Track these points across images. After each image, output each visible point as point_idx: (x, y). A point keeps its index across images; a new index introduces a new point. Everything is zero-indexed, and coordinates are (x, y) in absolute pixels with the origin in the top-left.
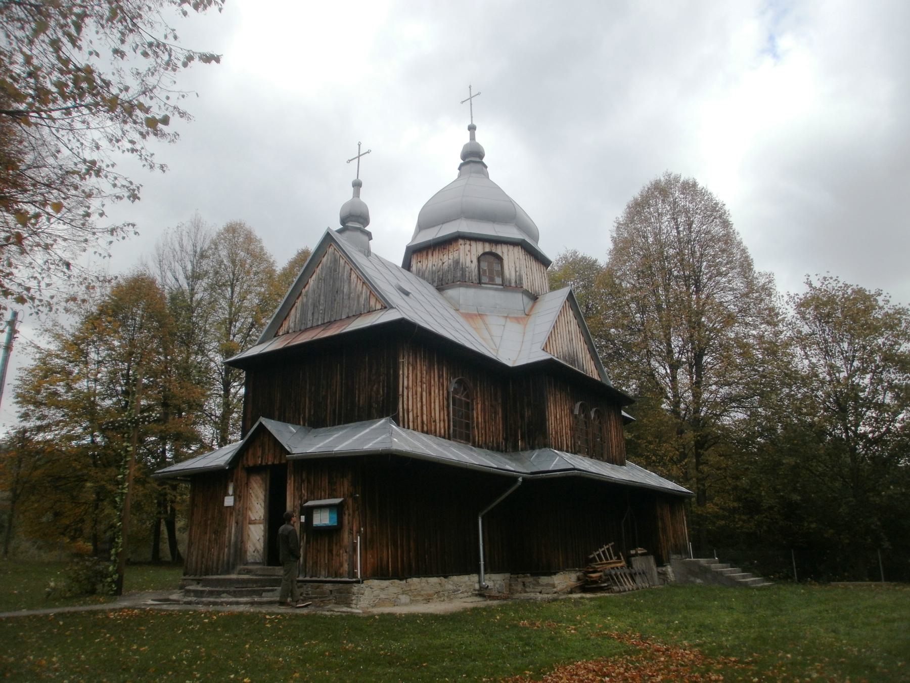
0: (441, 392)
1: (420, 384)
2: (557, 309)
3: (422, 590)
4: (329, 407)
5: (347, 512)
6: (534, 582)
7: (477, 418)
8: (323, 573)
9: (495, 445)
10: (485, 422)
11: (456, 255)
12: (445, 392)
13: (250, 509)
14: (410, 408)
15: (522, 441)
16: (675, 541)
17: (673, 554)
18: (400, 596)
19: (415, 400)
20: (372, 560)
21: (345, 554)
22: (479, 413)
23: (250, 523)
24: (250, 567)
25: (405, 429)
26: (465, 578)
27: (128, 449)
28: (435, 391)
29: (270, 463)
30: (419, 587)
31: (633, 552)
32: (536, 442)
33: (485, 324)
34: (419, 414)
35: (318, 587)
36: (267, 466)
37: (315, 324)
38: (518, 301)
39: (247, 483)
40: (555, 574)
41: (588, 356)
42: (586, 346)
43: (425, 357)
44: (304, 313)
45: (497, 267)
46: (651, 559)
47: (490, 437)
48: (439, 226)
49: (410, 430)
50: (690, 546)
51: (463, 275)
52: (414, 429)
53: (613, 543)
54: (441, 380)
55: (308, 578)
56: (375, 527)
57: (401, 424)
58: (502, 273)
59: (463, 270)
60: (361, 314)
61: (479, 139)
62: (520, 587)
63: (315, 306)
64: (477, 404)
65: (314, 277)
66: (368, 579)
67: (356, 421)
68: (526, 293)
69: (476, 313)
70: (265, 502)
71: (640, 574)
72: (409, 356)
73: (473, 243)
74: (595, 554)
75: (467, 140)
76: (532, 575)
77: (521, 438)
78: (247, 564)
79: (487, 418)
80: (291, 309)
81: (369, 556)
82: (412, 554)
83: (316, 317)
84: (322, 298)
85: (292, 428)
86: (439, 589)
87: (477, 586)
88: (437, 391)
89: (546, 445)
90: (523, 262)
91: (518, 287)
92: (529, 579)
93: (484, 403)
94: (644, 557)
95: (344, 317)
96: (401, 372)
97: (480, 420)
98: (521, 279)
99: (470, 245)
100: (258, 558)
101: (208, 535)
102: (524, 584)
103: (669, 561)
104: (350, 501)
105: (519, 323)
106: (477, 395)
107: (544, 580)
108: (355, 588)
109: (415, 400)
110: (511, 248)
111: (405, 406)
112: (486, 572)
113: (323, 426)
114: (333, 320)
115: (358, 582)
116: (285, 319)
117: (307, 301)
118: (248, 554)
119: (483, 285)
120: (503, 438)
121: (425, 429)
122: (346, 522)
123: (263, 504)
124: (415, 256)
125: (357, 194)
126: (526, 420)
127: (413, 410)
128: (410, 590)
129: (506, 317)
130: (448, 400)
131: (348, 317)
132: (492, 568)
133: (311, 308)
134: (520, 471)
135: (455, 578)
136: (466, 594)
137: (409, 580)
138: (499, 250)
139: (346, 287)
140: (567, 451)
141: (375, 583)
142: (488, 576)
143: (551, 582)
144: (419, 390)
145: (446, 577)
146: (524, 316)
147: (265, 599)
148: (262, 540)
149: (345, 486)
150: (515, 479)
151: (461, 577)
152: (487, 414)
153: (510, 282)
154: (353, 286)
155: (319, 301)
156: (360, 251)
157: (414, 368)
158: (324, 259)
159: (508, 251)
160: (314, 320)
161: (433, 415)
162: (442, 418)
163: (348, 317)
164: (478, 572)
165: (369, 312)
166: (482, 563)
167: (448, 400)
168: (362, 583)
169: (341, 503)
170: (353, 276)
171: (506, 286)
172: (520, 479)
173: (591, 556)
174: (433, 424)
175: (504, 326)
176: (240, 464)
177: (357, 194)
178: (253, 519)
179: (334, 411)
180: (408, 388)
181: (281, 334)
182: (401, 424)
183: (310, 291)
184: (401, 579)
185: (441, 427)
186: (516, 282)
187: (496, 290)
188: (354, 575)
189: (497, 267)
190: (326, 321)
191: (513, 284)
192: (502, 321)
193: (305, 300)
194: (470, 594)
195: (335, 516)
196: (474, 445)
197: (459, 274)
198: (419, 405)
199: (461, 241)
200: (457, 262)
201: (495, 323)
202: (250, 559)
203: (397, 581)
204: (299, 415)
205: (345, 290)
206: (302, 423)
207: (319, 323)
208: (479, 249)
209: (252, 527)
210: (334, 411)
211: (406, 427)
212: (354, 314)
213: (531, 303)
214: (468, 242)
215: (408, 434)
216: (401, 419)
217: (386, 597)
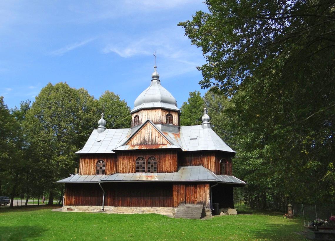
14: (83, 170)
26: (98, 207)
96: (80, 163)
111: (81, 170)
112: (106, 205)
135: (94, 206)
203: (75, 206)
211: (81, 174)
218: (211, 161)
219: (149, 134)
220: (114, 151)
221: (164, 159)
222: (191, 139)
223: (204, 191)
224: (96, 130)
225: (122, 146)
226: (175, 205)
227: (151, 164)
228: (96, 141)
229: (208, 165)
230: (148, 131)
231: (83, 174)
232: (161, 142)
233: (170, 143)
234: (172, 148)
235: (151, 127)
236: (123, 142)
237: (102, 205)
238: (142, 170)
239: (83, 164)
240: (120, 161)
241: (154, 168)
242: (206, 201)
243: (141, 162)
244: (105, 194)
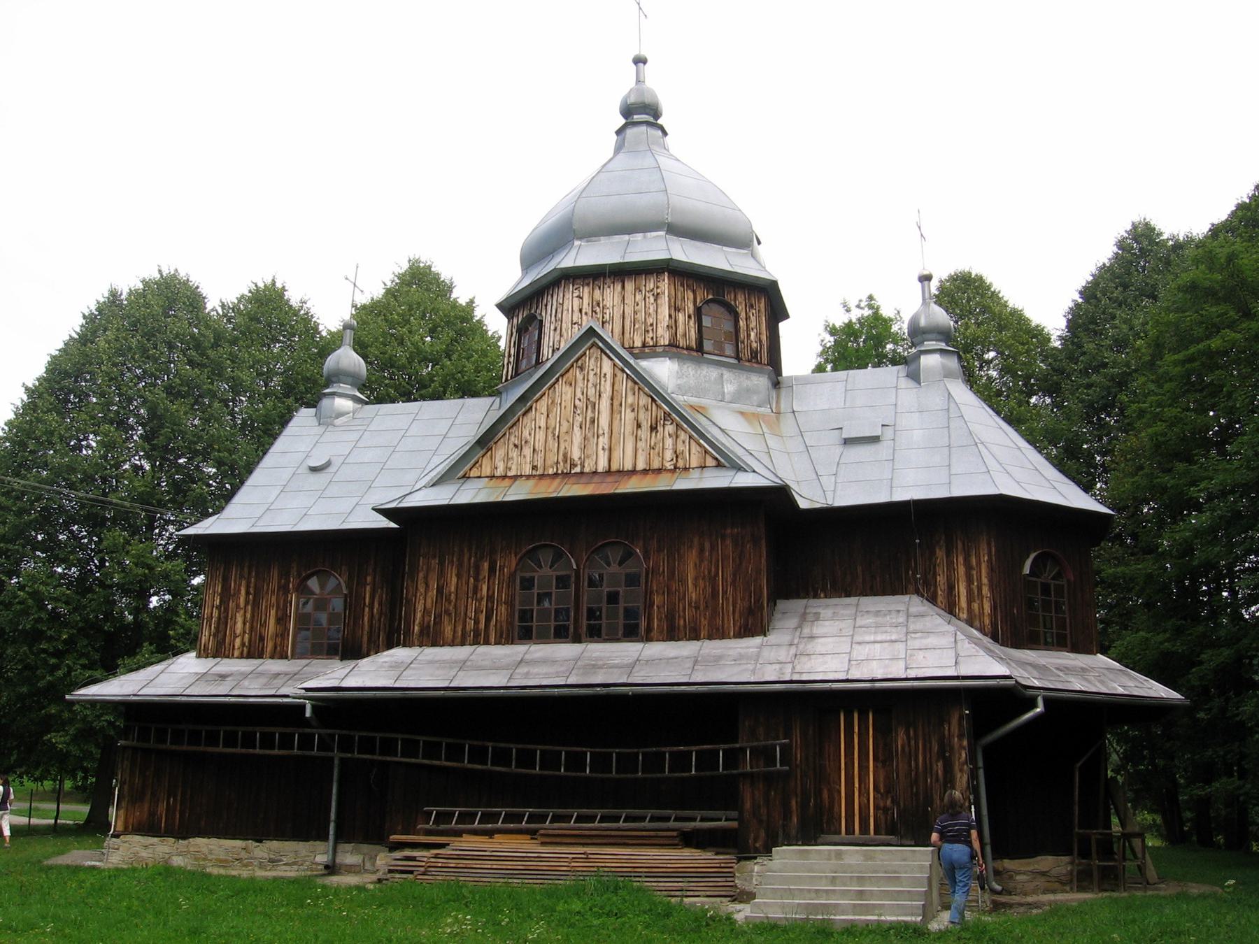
3: (211, 854)
30: (205, 850)
86: (243, 855)
112: (342, 837)
135: (275, 844)
137: (191, 840)
141: (137, 838)
151: (287, 843)
184: (184, 838)
203: (172, 840)
217: (151, 856)
218: (969, 568)
220: (387, 513)
222: (848, 442)
223: (936, 748)
224: (312, 411)
225: (432, 486)
226: (755, 840)
227: (606, 589)
228: (305, 466)
229: (951, 588)
230: (591, 392)
232: (669, 455)
233: (725, 461)
234: (733, 485)
235: (607, 366)
236: (440, 463)
237: (324, 838)
238: (553, 624)
241: (621, 611)
243: (546, 572)
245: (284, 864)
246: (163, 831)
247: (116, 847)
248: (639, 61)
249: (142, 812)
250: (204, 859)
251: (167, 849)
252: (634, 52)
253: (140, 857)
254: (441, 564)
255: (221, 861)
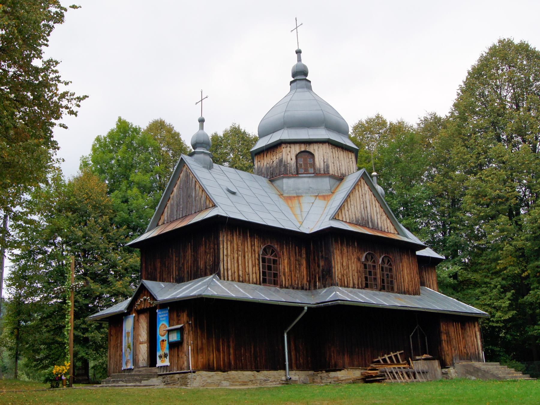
0: (253, 256)
1: (236, 252)
2: (349, 188)
3: (239, 379)
4: (185, 270)
5: (185, 332)
6: (327, 376)
7: (284, 269)
8: (175, 368)
9: (300, 286)
10: (291, 271)
11: (280, 155)
12: (257, 255)
13: (140, 335)
14: (229, 267)
15: (319, 282)
16: (466, 350)
17: (461, 359)
18: (223, 382)
19: (232, 263)
20: (202, 360)
21: (185, 357)
22: (286, 266)
23: (140, 344)
24: (140, 369)
25: (225, 281)
27: (69, 304)
28: (248, 255)
29: (148, 307)
31: (417, 358)
32: (327, 282)
33: (300, 203)
34: (236, 271)
35: (172, 377)
36: (147, 308)
37: (178, 218)
38: (325, 183)
39: (138, 320)
40: (340, 370)
41: (385, 217)
42: (382, 210)
43: (239, 234)
44: (172, 211)
45: (310, 161)
46: (436, 363)
47: (295, 281)
48: (271, 135)
49: (229, 282)
50: (482, 355)
51: (286, 169)
52: (232, 280)
53: (403, 351)
54: (253, 247)
55: (168, 372)
56: (204, 341)
57: (222, 278)
58: (313, 165)
59: (286, 166)
60: (202, 210)
61: (304, 62)
62: (319, 380)
63: (178, 205)
64: (284, 260)
65: (176, 186)
66: (199, 370)
67: (199, 277)
68: (333, 177)
69: (295, 195)
70: (147, 330)
71: (419, 373)
72: (227, 235)
73: (292, 146)
74: (380, 359)
75: (295, 62)
76: (327, 371)
77: (318, 280)
78: (139, 368)
79: (292, 268)
80: (165, 208)
81: (200, 357)
82: (232, 357)
83: (178, 213)
84: (181, 200)
85: (162, 285)
86: (253, 378)
87: (284, 378)
88: (250, 255)
89: (332, 285)
90: (330, 154)
91: (326, 173)
92: (324, 374)
93: (289, 259)
94: (428, 361)
95: (193, 212)
96: (221, 246)
97: (286, 270)
98: (328, 167)
99: (290, 147)
100: (145, 365)
101: (119, 353)
102: (321, 378)
103: (453, 365)
104: (186, 325)
105: (324, 199)
106: (283, 254)
107: (332, 374)
108: (190, 376)
109: (232, 263)
110: (321, 145)
111: (225, 267)
112: (291, 368)
113: (182, 282)
114: (187, 215)
115: (191, 372)
116: (162, 215)
117: (174, 202)
118: (140, 362)
119: (299, 175)
120: (307, 281)
121: (241, 279)
122: (185, 338)
123: (146, 332)
124: (256, 157)
125: (202, 127)
126: (321, 268)
127: (231, 269)
128: (230, 378)
129: (316, 196)
130: (259, 260)
131: (195, 213)
132: (296, 366)
133: (175, 206)
134: (308, 303)
135: (265, 372)
136: (274, 383)
137: (229, 372)
138: (311, 148)
139: (194, 193)
140: (354, 287)
141: (204, 373)
142: (293, 372)
143: (336, 376)
144: (236, 256)
145: (258, 371)
146: (330, 193)
147: (142, 384)
148: (146, 354)
149: (184, 317)
150: (302, 308)
151: (270, 372)
152: (292, 266)
153: (320, 170)
154: (197, 193)
155: (180, 202)
156: (204, 167)
157: (232, 242)
158: (181, 175)
159: (319, 148)
160: (178, 215)
161: (247, 270)
162: (254, 271)
163: (195, 213)
164: (284, 369)
165: (206, 209)
166: (287, 363)
167: (259, 260)
168: (194, 372)
169: (182, 327)
170: (197, 186)
171: (317, 174)
172: (306, 308)
173: (376, 360)
174: (247, 276)
175: (313, 203)
176: (133, 310)
177: (202, 127)
178: (142, 341)
179: (188, 272)
180: (227, 255)
181: (160, 224)
182: (222, 278)
183: (175, 196)
184: (224, 371)
185: (253, 277)
186: (324, 170)
187: (309, 177)
188: (189, 368)
189: (310, 161)
190: (184, 215)
191: (322, 172)
192: (312, 199)
193: (172, 202)
194: (278, 383)
195: (179, 335)
196: (281, 287)
197: (283, 169)
198: (236, 265)
199: (284, 146)
200: (281, 161)
201: (306, 201)
202: (141, 365)
204: (170, 275)
205: (193, 195)
206: (172, 280)
207: (180, 217)
208: (296, 149)
209: (141, 345)
210: (188, 272)
211: (226, 279)
212: (198, 210)
213: (338, 183)
214: (289, 145)
215: (220, 283)
216: (222, 275)
217: (212, 381)
219: (366, 203)
221: (401, 264)
231: (230, 278)
239: (227, 249)
240: (336, 256)
242: (479, 353)
244: (287, 337)
245: (270, 382)
246: (215, 369)
247: (195, 378)
248: (299, 52)
249: (201, 360)
250: (236, 382)
251: (219, 378)
252: (297, 49)
253: (207, 383)
254: (341, 252)
255: (243, 382)
